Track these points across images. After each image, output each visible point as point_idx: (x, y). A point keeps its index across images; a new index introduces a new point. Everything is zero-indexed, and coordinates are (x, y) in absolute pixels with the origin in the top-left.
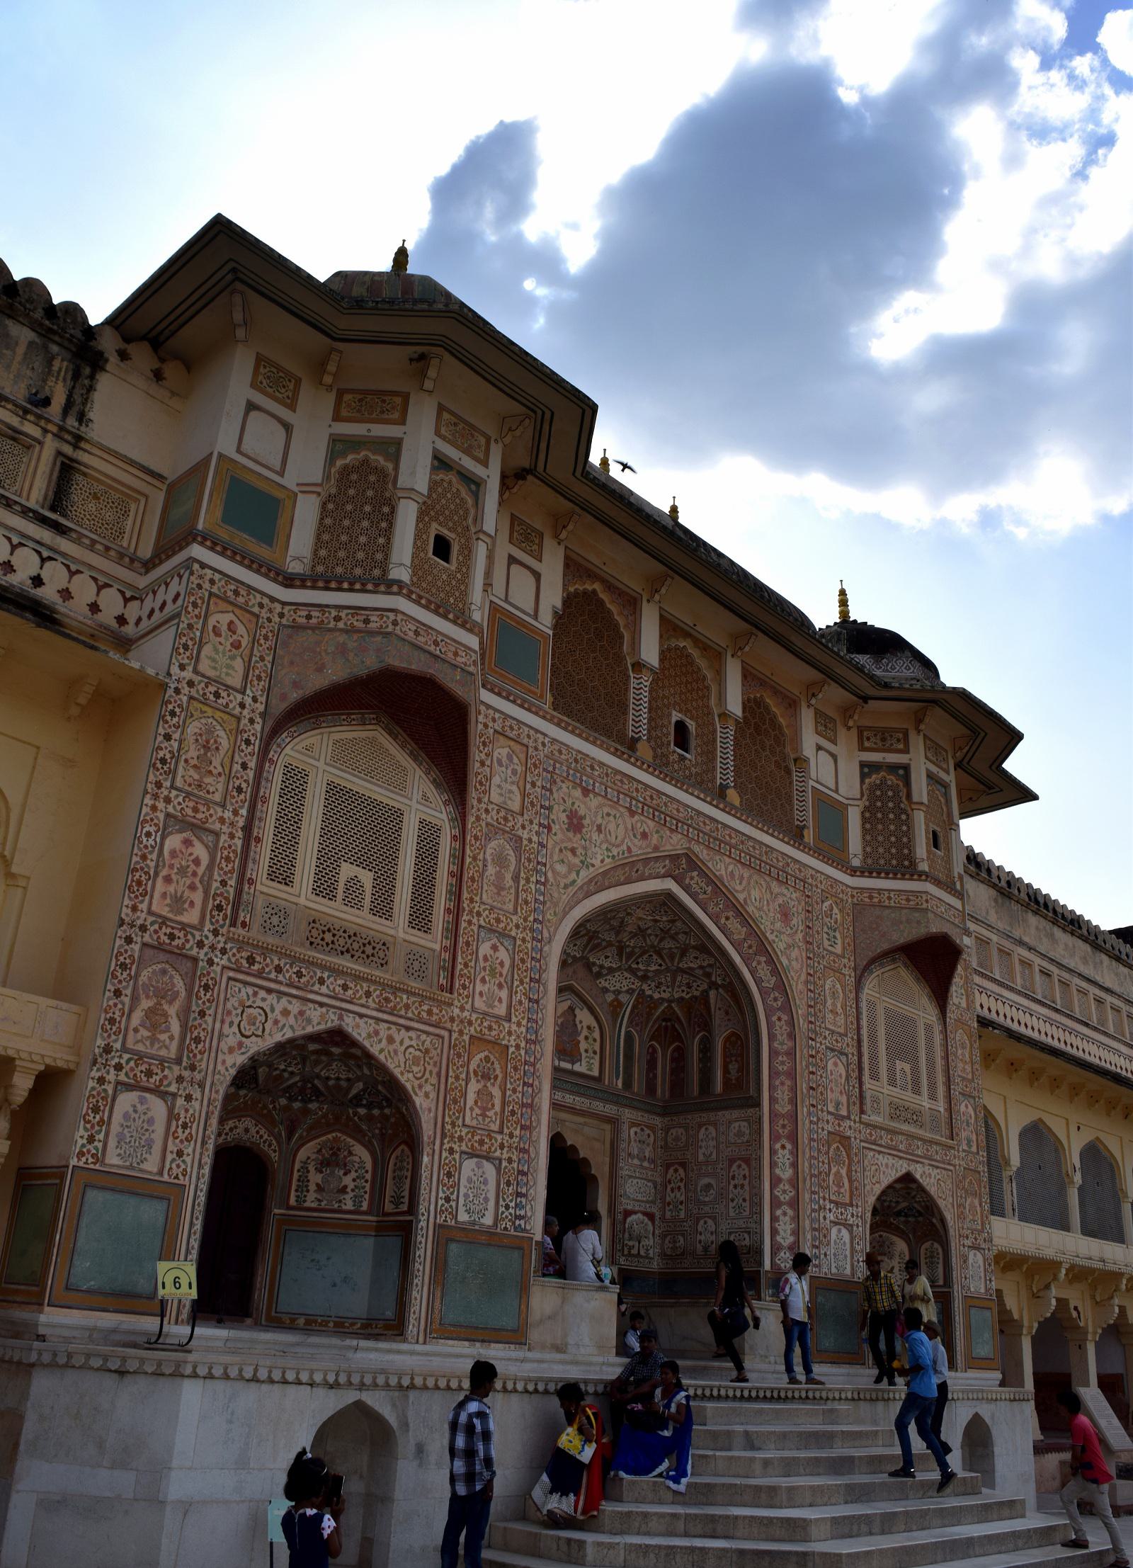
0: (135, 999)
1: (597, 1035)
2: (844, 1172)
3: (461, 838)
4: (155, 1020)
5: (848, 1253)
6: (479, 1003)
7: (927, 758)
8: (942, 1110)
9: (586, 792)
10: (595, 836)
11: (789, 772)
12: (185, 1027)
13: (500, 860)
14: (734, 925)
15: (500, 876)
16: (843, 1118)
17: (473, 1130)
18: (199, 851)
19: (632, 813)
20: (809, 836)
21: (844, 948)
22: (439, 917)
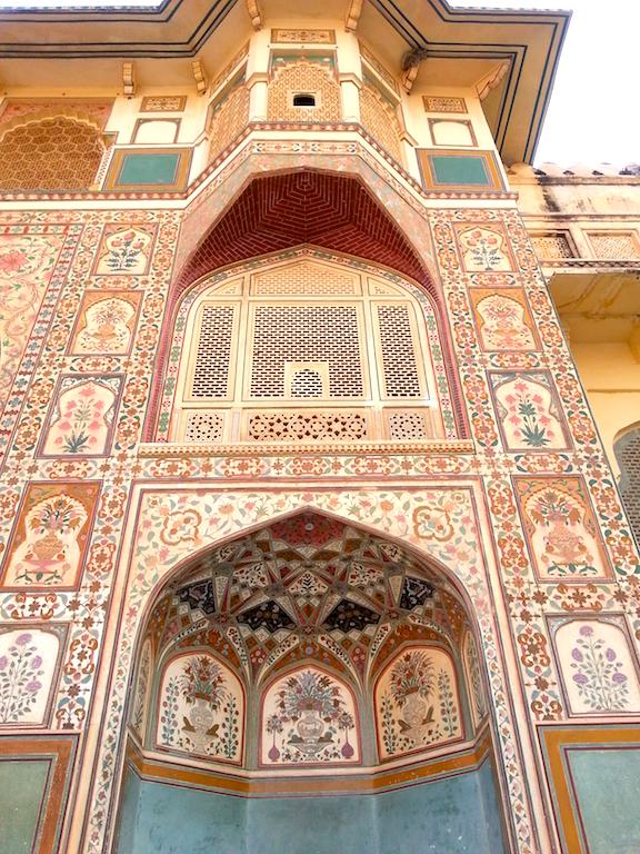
2: (69, 539)
5: (46, 681)
8: (434, 404)
16: (85, 458)
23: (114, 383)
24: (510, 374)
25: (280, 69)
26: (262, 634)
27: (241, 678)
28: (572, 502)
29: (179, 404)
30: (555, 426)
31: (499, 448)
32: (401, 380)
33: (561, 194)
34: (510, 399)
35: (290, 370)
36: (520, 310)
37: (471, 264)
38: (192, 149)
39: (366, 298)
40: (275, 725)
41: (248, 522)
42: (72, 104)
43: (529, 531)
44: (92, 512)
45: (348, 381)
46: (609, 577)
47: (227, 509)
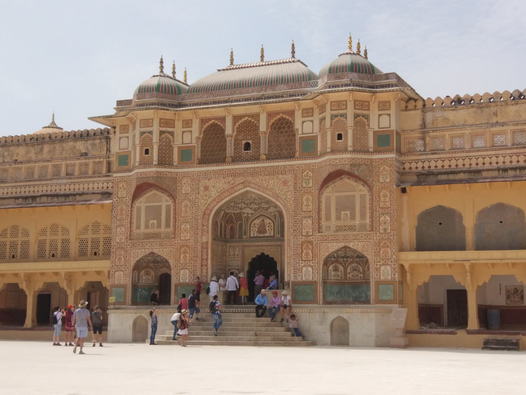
0: (116, 257)
1: (272, 224)
2: (310, 251)
3: (175, 206)
4: (120, 259)
5: (311, 274)
6: (182, 238)
7: (331, 110)
8: (368, 222)
9: (209, 180)
10: (213, 189)
11: (294, 135)
12: (124, 259)
13: (186, 206)
14: (268, 192)
15: (186, 209)
16: (309, 236)
17: (182, 264)
18: (123, 229)
19: (224, 178)
20: (297, 154)
21: (313, 184)
22: (172, 224)
23: (311, 218)
24: (383, 214)
25: (334, 121)
26: (345, 259)
27: (343, 266)
28: (389, 244)
29: (323, 223)
30: (389, 227)
31: (378, 233)
32: (363, 217)
33: (429, 116)
34: (382, 221)
35: (343, 213)
36: (389, 194)
37: (381, 180)
38: (317, 136)
39: (357, 192)
40: (349, 273)
41: (336, 248)
42: (284, 113)
43: (380, 250)
44: (312, 246)
45: (353, 217)
46: (391, 259)
47: (333, 246)
